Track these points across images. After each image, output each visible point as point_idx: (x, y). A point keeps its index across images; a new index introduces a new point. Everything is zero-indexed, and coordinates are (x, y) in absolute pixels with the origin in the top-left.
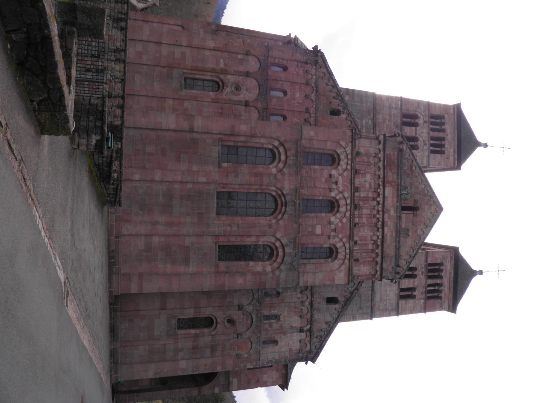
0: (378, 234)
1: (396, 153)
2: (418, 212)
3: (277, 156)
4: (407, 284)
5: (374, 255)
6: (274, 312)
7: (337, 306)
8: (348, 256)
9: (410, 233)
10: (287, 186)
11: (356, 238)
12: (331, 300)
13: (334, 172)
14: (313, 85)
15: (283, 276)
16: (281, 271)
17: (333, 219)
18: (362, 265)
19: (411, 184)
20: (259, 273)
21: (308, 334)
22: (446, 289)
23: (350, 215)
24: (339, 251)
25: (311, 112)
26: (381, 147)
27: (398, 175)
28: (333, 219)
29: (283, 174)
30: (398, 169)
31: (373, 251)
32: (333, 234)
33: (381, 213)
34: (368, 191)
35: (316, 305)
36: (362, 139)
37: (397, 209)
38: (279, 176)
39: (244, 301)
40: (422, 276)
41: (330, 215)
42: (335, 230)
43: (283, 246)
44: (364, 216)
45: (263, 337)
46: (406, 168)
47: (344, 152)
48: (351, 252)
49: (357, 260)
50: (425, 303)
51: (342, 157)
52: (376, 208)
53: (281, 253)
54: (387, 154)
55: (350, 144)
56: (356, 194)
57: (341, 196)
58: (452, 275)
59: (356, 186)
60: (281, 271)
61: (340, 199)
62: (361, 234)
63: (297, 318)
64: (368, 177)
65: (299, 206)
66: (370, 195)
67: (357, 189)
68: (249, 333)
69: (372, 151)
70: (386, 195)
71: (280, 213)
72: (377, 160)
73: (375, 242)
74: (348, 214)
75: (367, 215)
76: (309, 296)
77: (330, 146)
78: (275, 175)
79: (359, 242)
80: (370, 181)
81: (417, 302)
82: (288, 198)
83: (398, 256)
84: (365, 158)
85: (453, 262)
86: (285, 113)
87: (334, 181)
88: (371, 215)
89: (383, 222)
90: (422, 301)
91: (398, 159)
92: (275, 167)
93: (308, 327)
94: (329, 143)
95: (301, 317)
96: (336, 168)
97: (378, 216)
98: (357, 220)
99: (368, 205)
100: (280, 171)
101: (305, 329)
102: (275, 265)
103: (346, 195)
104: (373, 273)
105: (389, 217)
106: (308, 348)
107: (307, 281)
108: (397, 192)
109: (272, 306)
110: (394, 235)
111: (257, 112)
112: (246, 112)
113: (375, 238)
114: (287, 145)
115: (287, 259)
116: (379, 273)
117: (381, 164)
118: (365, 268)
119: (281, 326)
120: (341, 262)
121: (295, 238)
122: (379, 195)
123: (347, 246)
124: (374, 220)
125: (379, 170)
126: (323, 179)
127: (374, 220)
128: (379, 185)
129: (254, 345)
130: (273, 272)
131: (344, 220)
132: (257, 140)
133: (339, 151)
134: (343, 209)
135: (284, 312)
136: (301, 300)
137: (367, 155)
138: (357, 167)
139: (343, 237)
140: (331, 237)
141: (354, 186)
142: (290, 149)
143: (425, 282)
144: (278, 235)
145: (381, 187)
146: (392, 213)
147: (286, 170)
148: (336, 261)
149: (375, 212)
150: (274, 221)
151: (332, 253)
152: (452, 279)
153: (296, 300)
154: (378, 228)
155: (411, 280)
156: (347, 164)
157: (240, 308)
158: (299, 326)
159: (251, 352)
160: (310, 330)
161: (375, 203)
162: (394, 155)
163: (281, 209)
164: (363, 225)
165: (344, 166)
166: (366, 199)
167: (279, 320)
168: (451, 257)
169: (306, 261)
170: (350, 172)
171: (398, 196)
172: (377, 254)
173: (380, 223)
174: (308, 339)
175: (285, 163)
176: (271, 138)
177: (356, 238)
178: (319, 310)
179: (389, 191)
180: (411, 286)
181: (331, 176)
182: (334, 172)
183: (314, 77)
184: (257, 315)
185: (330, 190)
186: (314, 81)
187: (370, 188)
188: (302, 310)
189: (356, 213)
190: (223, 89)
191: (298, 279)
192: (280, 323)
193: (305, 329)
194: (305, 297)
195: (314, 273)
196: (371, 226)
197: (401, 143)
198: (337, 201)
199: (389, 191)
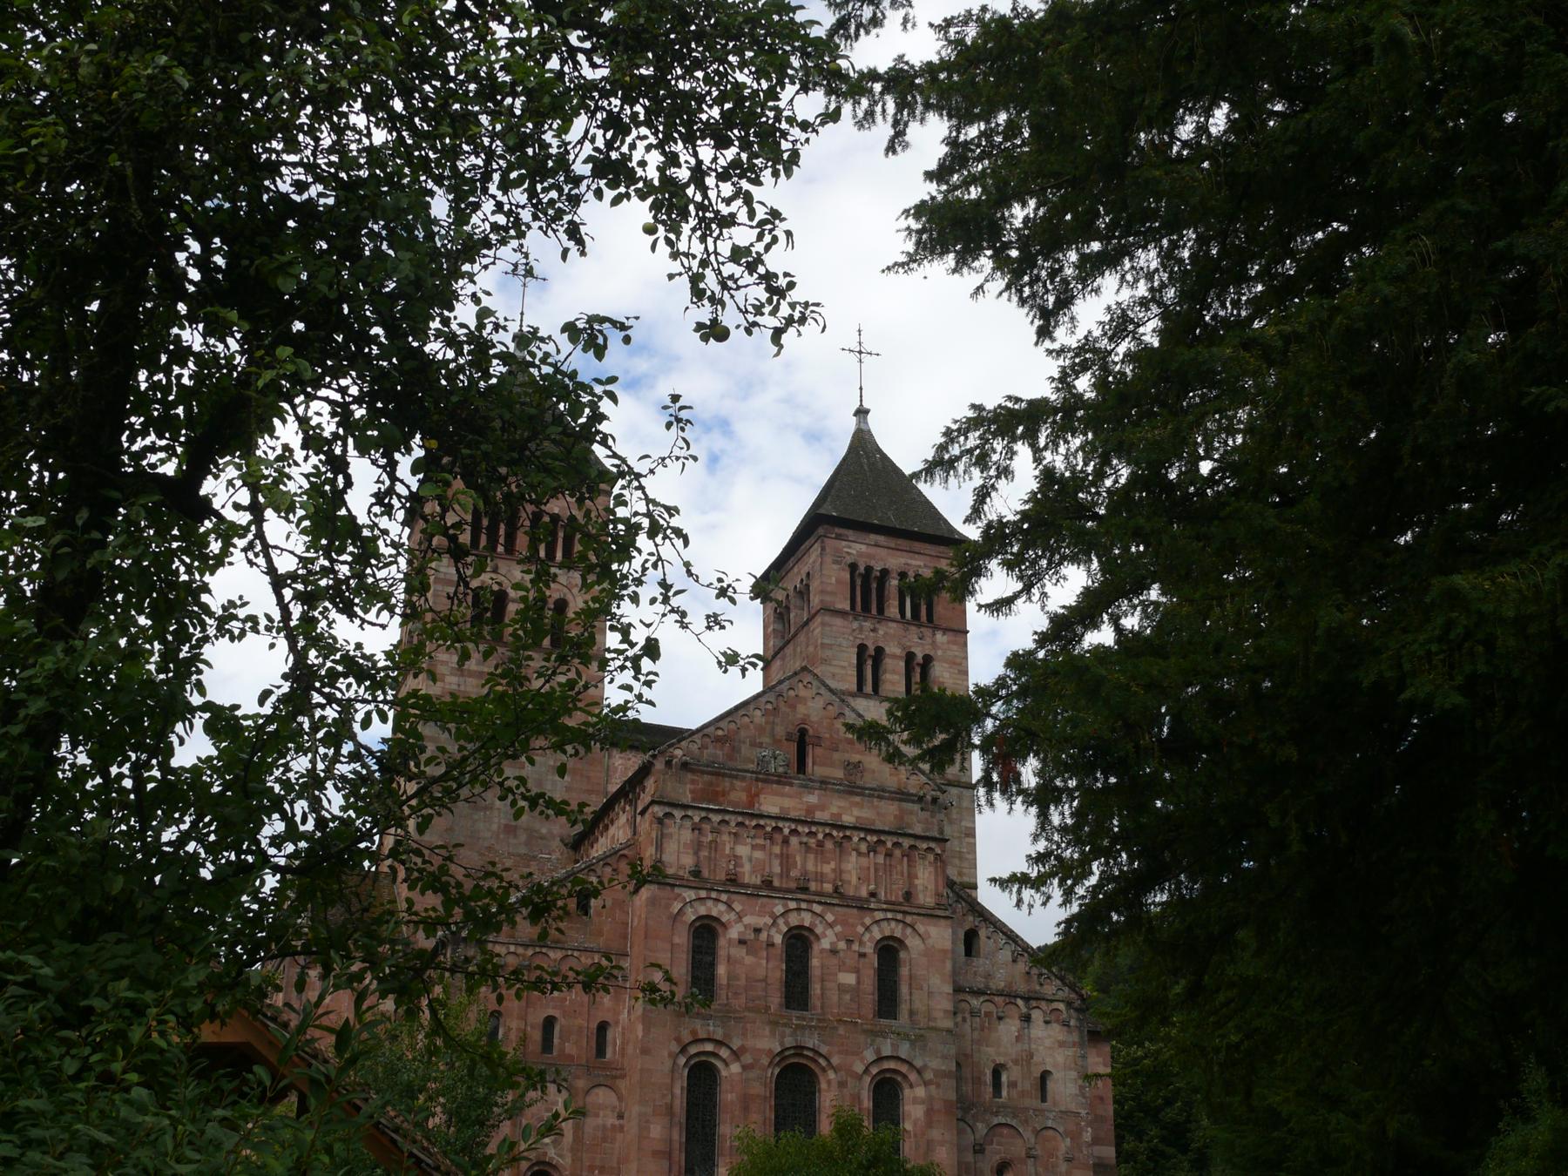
0: (856, 839)
1: (690, 776)
2: (811, 732)
3: (703, 1058)
4: (896, 677)
5: (898, 853)
6: (988, 1078)
7: (983, 933)
8: (900, 916)
9: (856, 758)
10: (766, 1042)
11: (864, 893)
12: (970, 941)
13: (734, 933)
14: (530, 952)
15: (935, 1063)
16: (925, 1067)
17: (825, 944)
18: (917, 882)
19: (754, 744)
20: (929, 1112)
21: (1034, 1004)
22: (914, 562)
23: (820, 903)
24: (887, 933)
25: (589, 962)
26: (678, 813)
27: (736, 777)
28: (825, 944)
29: (743, 1049)
30: (724, 775)
31: (889, 855)
32: (855, 947)
33: (814, 829)
35: (979, 983)
36: (665, 858)
37: (805, 787)
38: (747, 1059)
39: (970, 1138)
40: (881, 632)
41: (816, 948)
42: (849, 942)
43: (880, 1059)
45: (1033, 1102)
46: (719, 753)
47: (693, 905)
48: (892, 906)
49: (908, 896)
50: (945, 630)
51: (703, 911)
52: (805, 839)
53: (892, 1065)
54: (693, 800)
55: (677, 890)
56: (776, 883)
57: (781, 921)
58: (881, 539)
59: (759, 882)
60: (925, 1067)
61: (786, 923)
62: (854, 880)
63: (1002, 1027)
64: (743, 850)
65: (804, 1019)
66: (777, 850)
67: (767, 884)
68: (1028, 1134)
69: (687, 835)
70: (774, 810)
71: (816, 1061)
72: (706, 827)
73: (872, 849)
74: (817, 908)
76: (961, 997)
77: (682, 938)
78: (744, 1068)
79: (872, 887)
80: (748, 848)
81: (939, 653)
82: (789, 1042)
83: (901, 795)
84: (704, 853)
85: (850, 533)
86: (594, 1025)
87: (752, 936)
89: (833, 826)
90: (940, 637)
91: (703, 772)
92: (727, 1065)
93: (1020, 1002)
94: (677, 940)
95: (1000, 1018)
96: (723, 925)
97: (820, 836)
98: (828, 887)
99: (798, 859)
100: (736, 1055)
101: (1024, 1010)
102: (913, 1077)
103: (779, 909)
104: (931, 857)
105: (822, 808)
106: (1061, 1006)
107: (946, 1011)
108: (773, 782)
109: (977, 1081)
110: (858, 799)
111: (596, 1090)
112: (597, 1115)
113: (863, 847)
114: (687, 1038)
115: (904, 1050)
116: (933, 845)
117: (716, 818)
118: (920, 875)
119: (1016, 1062)
120: (909, 930)
121: (865, 1031)
122: (777, 829)
123: (879, 915)
124: (829, 845)
125: (727, 823)
126: (749, 960)
127: (829, 845)
128: (758, 826)
129: (1050, 1123)
130: (926, 1084)
131: (830, 917)
132: (677, 1102)
133: (690, 916)
134: (807, 919)
135: (990, 1054)
136: (967, 1015)
137: (697, 847)
138: (722, 877)
139: (863, 924)
140: (863, 950)
141: (760, 888)
142: (694, 1032)
143: (894, 625)
144: (859, 1068)
145: (762, 822)
146: (813, 799)
147: (736, 1044)
148: (907, 942)
149: (812, 842)
150: (831, 1075)
151: (889, 951)
152: (892, 542)
153: (967, 1026)
154: (845, 837)
155: (888, 663)
156: (717, 900)
157: (979, 1149)
158: (1017, 1022)
159: (1061, 1129)
160: (1027, 999)
161: (794, 840)
162: (693, 782)
163: (807, 1057)
164: (839, 872)
165: (722, 907)
166: (786, 860)
167: (1002, 1066)
168: (839, 537)
169: (904, 1009)
170: (734, 897)
171: (778, 783)
172: (896, 844)
173: (835, 833)
174: (1043, 1004)
175: (719, 1043)
176: (673, 1071)
177: (864, 893)
178: (988, 976)
179: (771, 804)
180: (903, 664)
181: (742, 942)
182: (734, 933)
183: (512, 948)
184: (996, 1114)
185: (771, 945)
186: (520, 950)
187: (763, 848)
188: (988, 1014)
189: (813, 886)
190: (550, 1164)
191: (941, 1030)
192: (1010, 1064)
193: (1024, 1010)
194: (963, 1005)
195: (930, 994)
197: (668, 763)
198: (790, 930)
199: (771, 804)
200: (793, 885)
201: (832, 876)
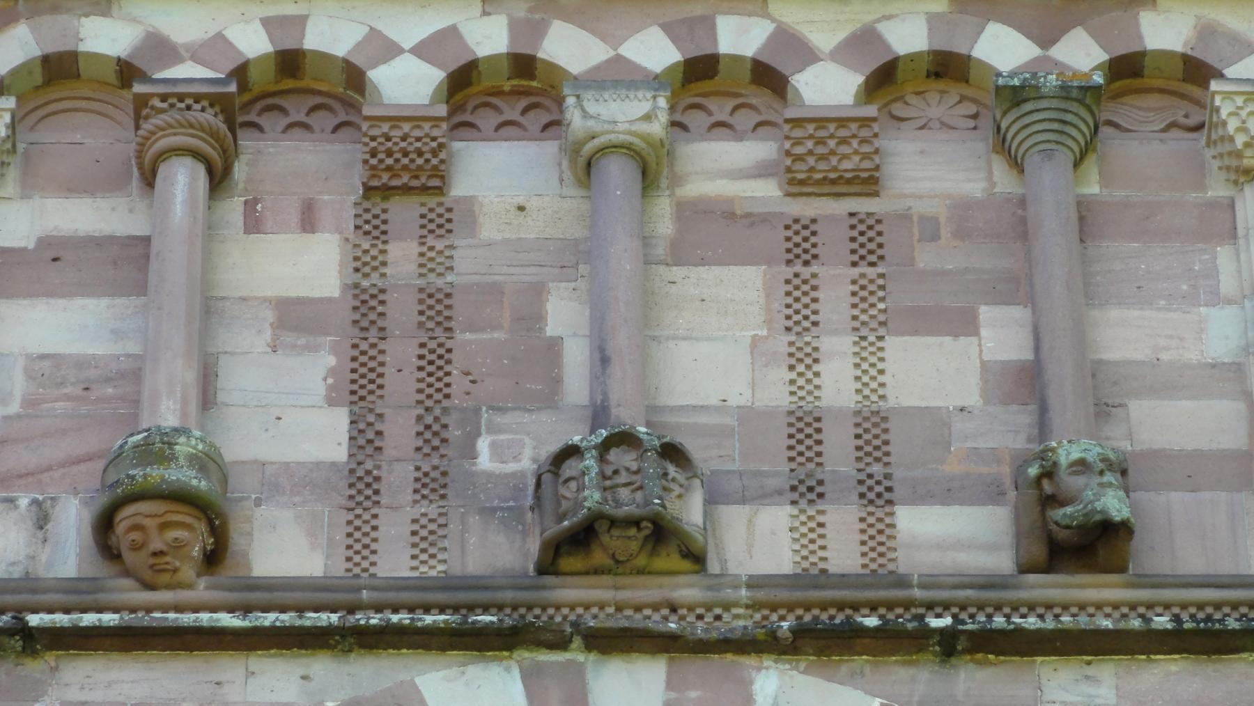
34: (209, 310)
44: (837, 385)
52: (630, 115)
56: (285, 547)
75: (799, 313)
88: (801, 245)
99: (564, 315)
149: (729, 166)
154: (1128, 69)
187: (125, 265)
196: (1087, 221)
200: (494, 551)
201: (1007, 433)
